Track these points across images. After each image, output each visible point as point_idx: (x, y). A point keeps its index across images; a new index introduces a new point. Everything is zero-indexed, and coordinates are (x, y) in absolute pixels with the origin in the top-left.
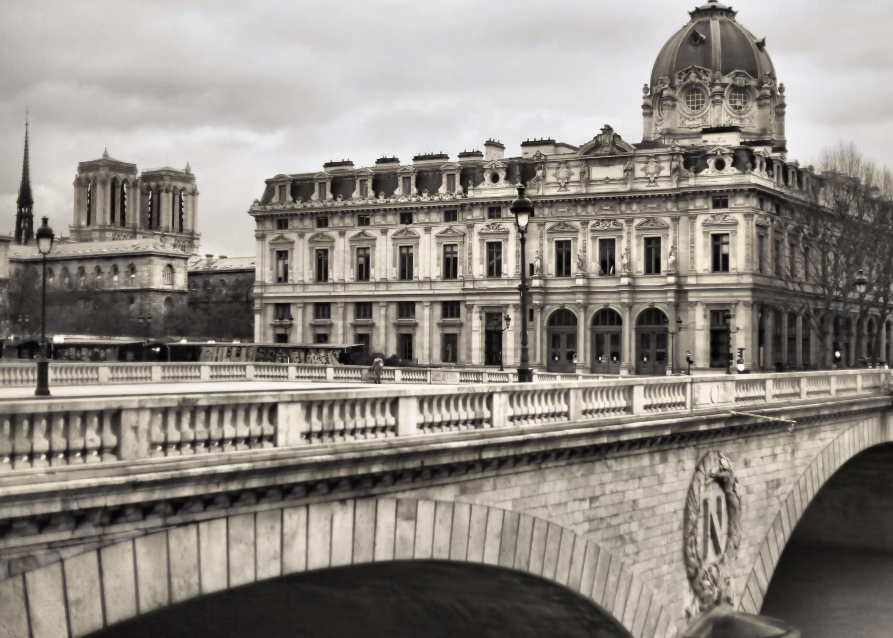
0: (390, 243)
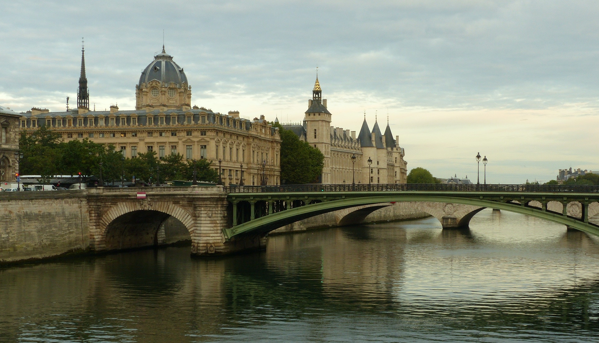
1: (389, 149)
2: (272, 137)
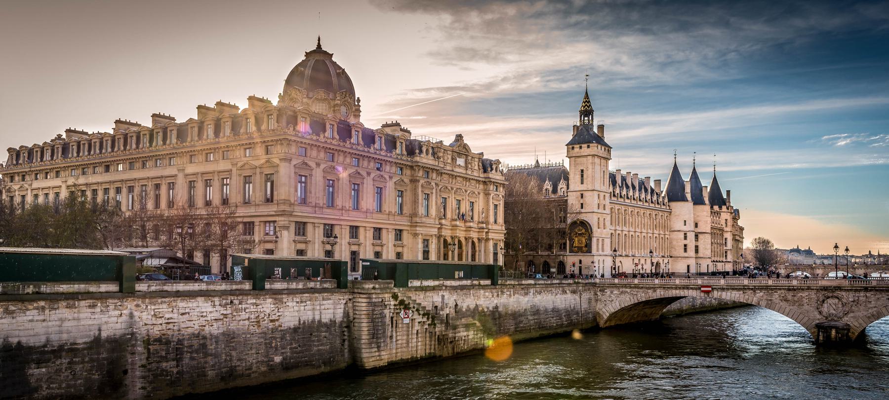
0: (372, 183)
1: (716, 208)
2: (486, 175)
